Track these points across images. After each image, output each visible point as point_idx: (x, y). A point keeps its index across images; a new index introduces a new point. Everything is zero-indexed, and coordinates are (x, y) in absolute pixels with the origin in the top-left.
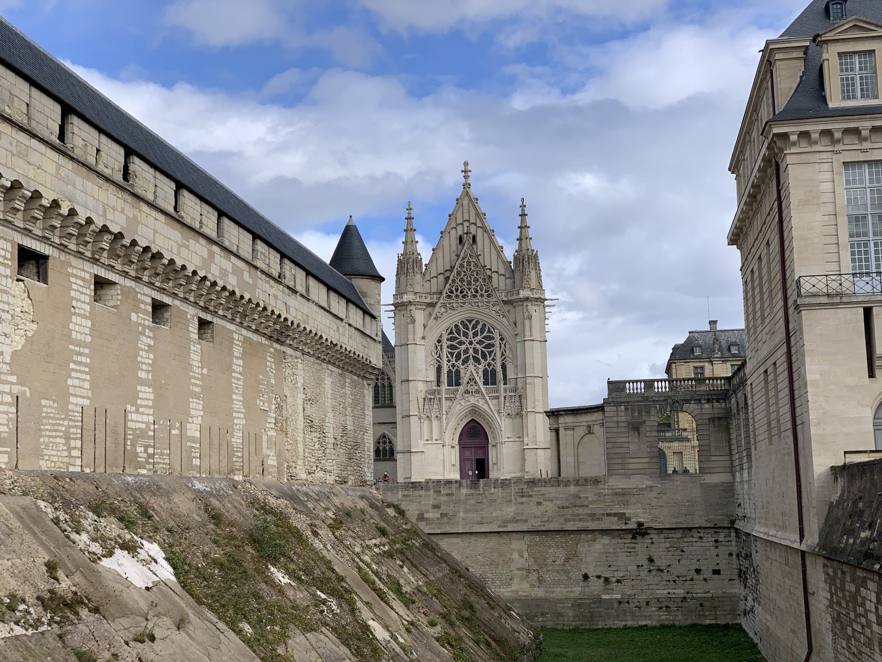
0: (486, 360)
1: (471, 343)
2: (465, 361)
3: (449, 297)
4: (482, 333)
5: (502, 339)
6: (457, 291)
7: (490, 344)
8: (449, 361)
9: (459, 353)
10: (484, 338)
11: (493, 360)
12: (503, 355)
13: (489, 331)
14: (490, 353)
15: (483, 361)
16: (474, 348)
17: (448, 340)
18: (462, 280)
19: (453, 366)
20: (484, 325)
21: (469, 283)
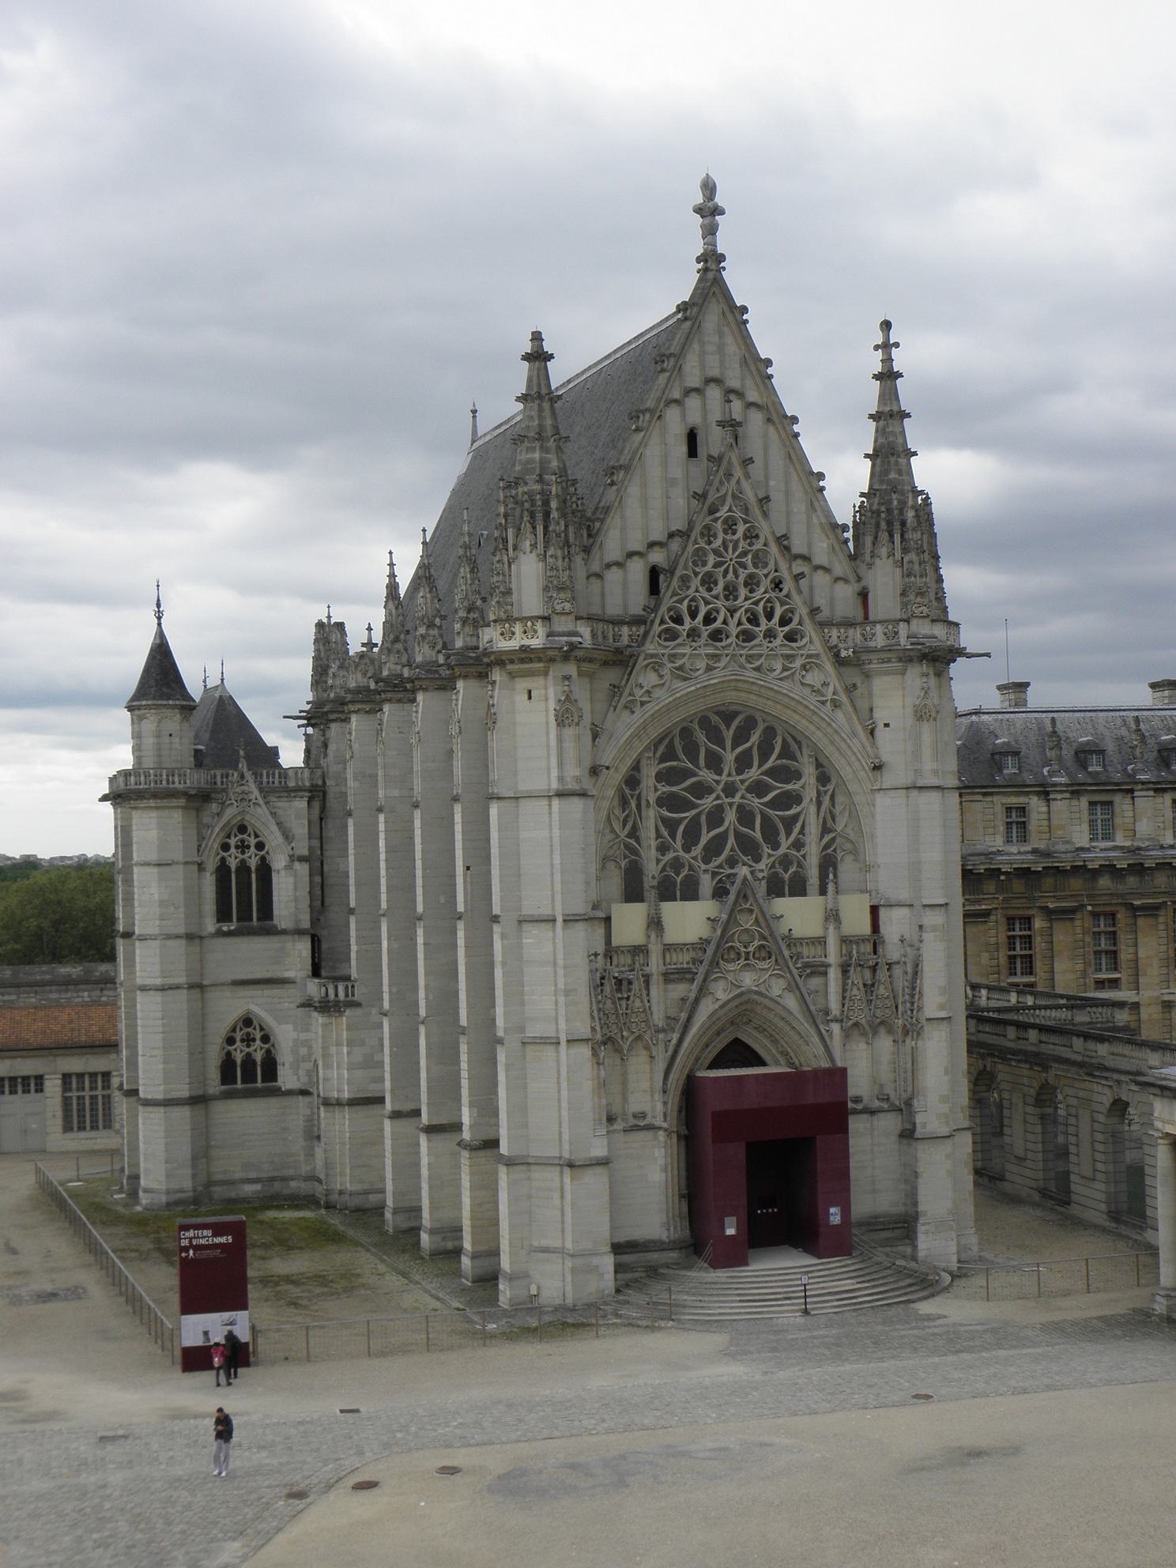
0: (776, 846)
1: (730, 790)
2: (714, 848)
3: (671, 635)
4: (764, 756)
5: (823, 779)
6: (693, 615)
7: (787, 794)
8: (663, 849)
9: (695, 823)
10: (769, 773)
11: (798, 845)
12: (825, 830)
13: (786, 753)
14: (790, 823)
15: (766, 850)
16: (741, 808)
17: (660, 777)
18: (709, 581)
19: (677, 864)
20: (770, 733)
21: (730, 592)
